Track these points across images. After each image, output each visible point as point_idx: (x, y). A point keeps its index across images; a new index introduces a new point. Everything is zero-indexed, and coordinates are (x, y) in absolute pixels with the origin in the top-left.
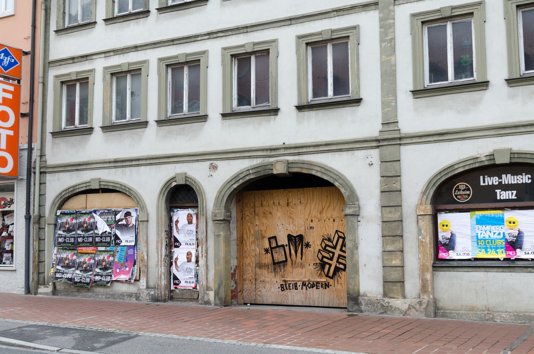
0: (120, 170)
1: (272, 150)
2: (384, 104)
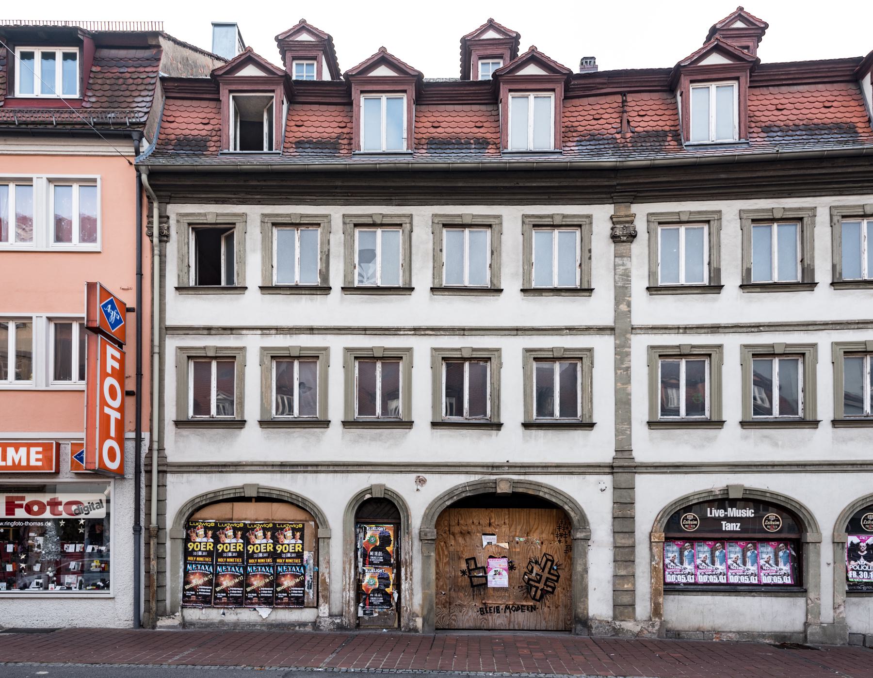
0: (289, 475)
1: (493, 467)
2: (618, 432)
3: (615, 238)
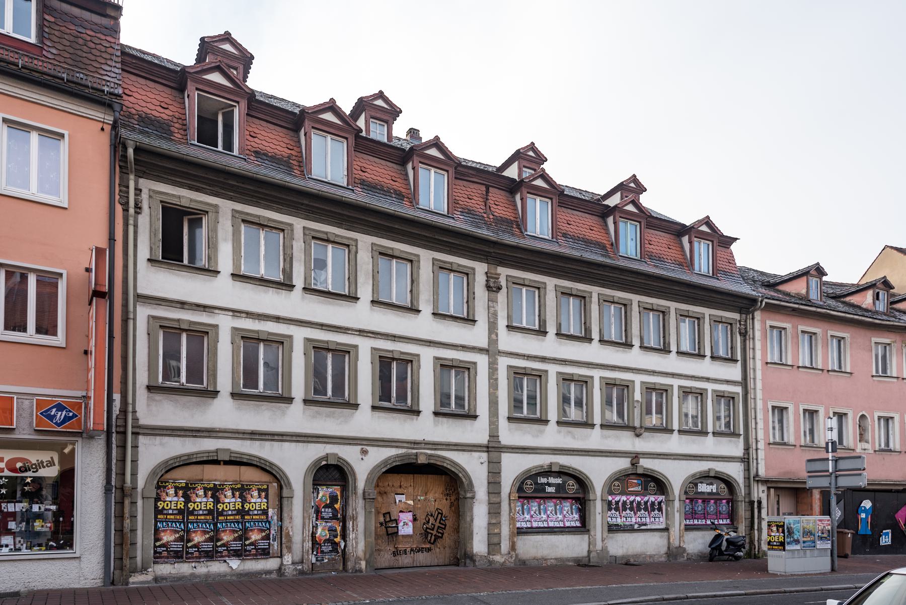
0: (258, 443)
3: (488, 288)
